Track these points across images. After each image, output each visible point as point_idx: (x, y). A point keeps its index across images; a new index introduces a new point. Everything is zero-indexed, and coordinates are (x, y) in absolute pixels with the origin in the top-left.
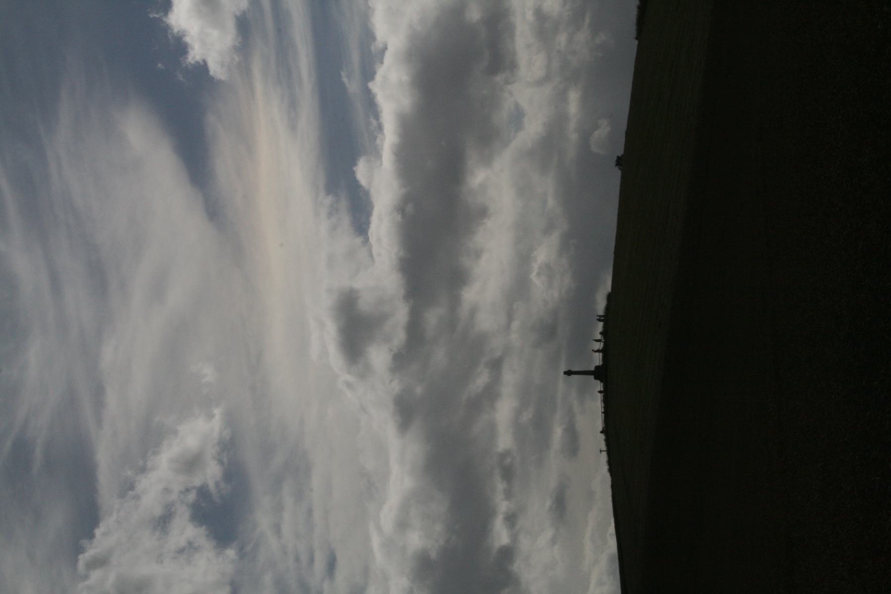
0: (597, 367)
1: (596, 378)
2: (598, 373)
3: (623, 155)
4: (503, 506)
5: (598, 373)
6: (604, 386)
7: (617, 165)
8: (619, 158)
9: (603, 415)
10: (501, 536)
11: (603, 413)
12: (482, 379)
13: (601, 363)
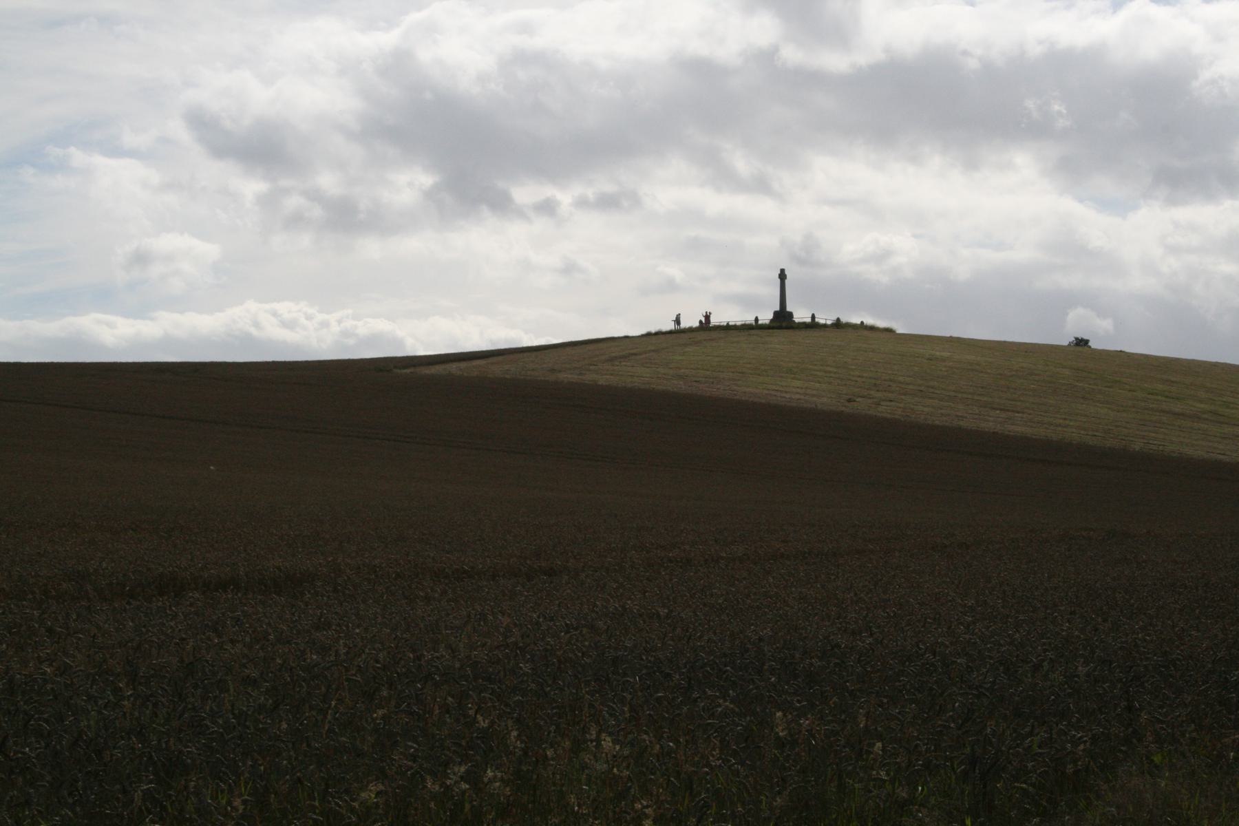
0: (791, 315)
1: (776, 313)
2: (783, 318)
3: (1090, 347)
4: (565, 197)
5: (783, 318)
6: (766, 324)
7: (1077, 339)
8: (1086, 342)
9: (725, 324)
10: (525, 193)
11: (728, 324)
12: (742, 164)
13: (797, 320)
